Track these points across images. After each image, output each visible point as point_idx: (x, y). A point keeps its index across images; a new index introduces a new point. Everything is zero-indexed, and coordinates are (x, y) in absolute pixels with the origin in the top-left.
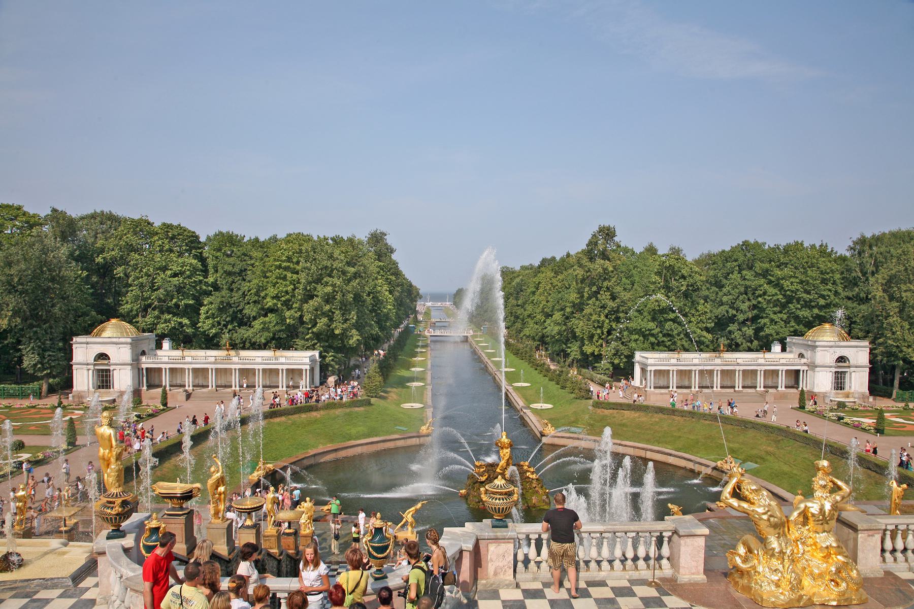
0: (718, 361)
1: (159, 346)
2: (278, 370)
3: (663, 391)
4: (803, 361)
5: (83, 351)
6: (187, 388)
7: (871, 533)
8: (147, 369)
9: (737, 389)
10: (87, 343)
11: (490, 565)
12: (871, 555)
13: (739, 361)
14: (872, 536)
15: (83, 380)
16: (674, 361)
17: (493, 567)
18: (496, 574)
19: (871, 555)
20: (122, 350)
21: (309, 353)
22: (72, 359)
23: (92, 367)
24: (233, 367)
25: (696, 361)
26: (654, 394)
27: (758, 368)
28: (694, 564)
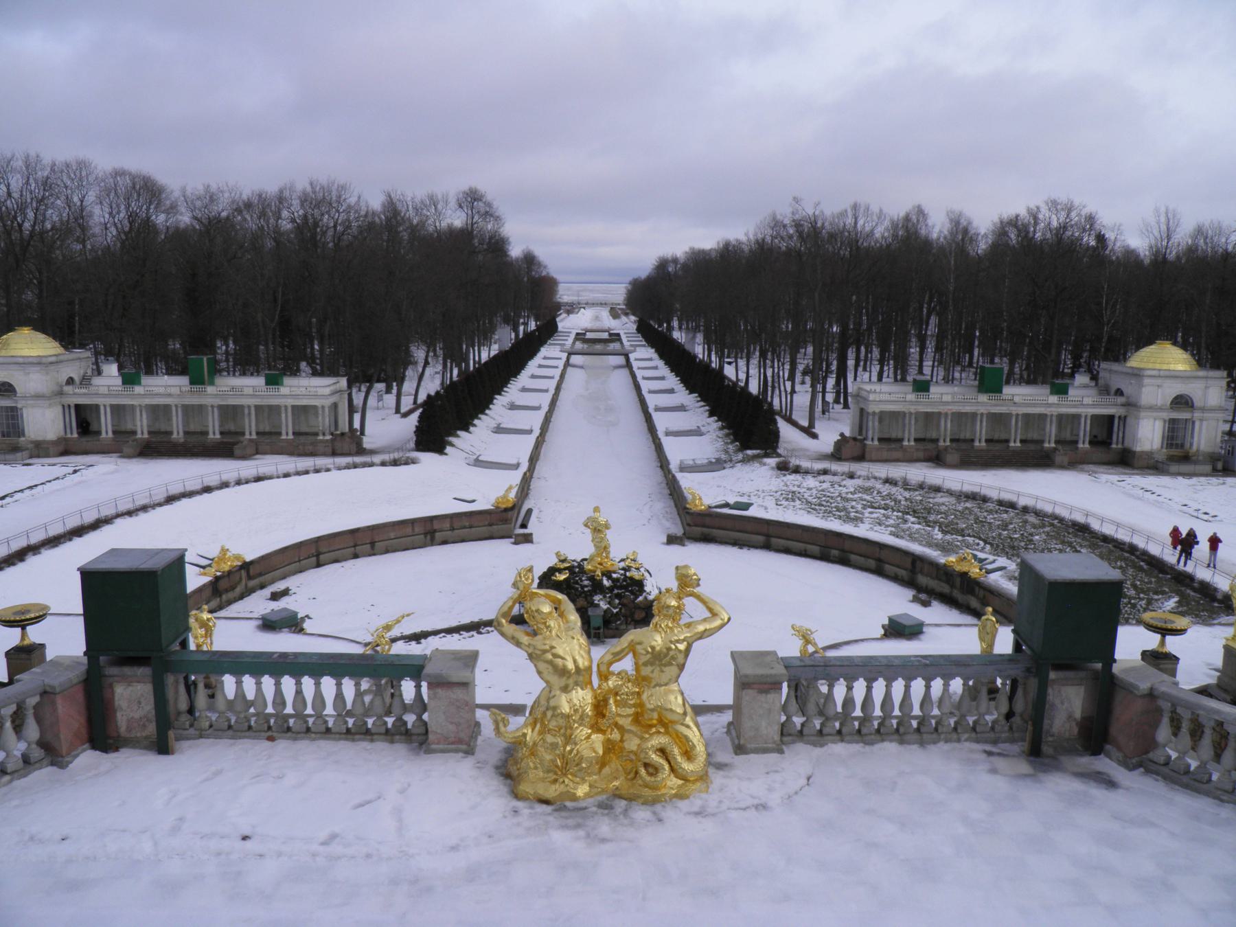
1: (99, 372)
2: (278, 407)
4: (1121, 400)
6: (139, 436)
11: (119, 715)
12: (764, 724)
13: (1016, 399)
14: (766, 692)
17: (125, 718)
18: (129, 729)
19: (764, 724)
25: (946, 398)
28: (452, 727)
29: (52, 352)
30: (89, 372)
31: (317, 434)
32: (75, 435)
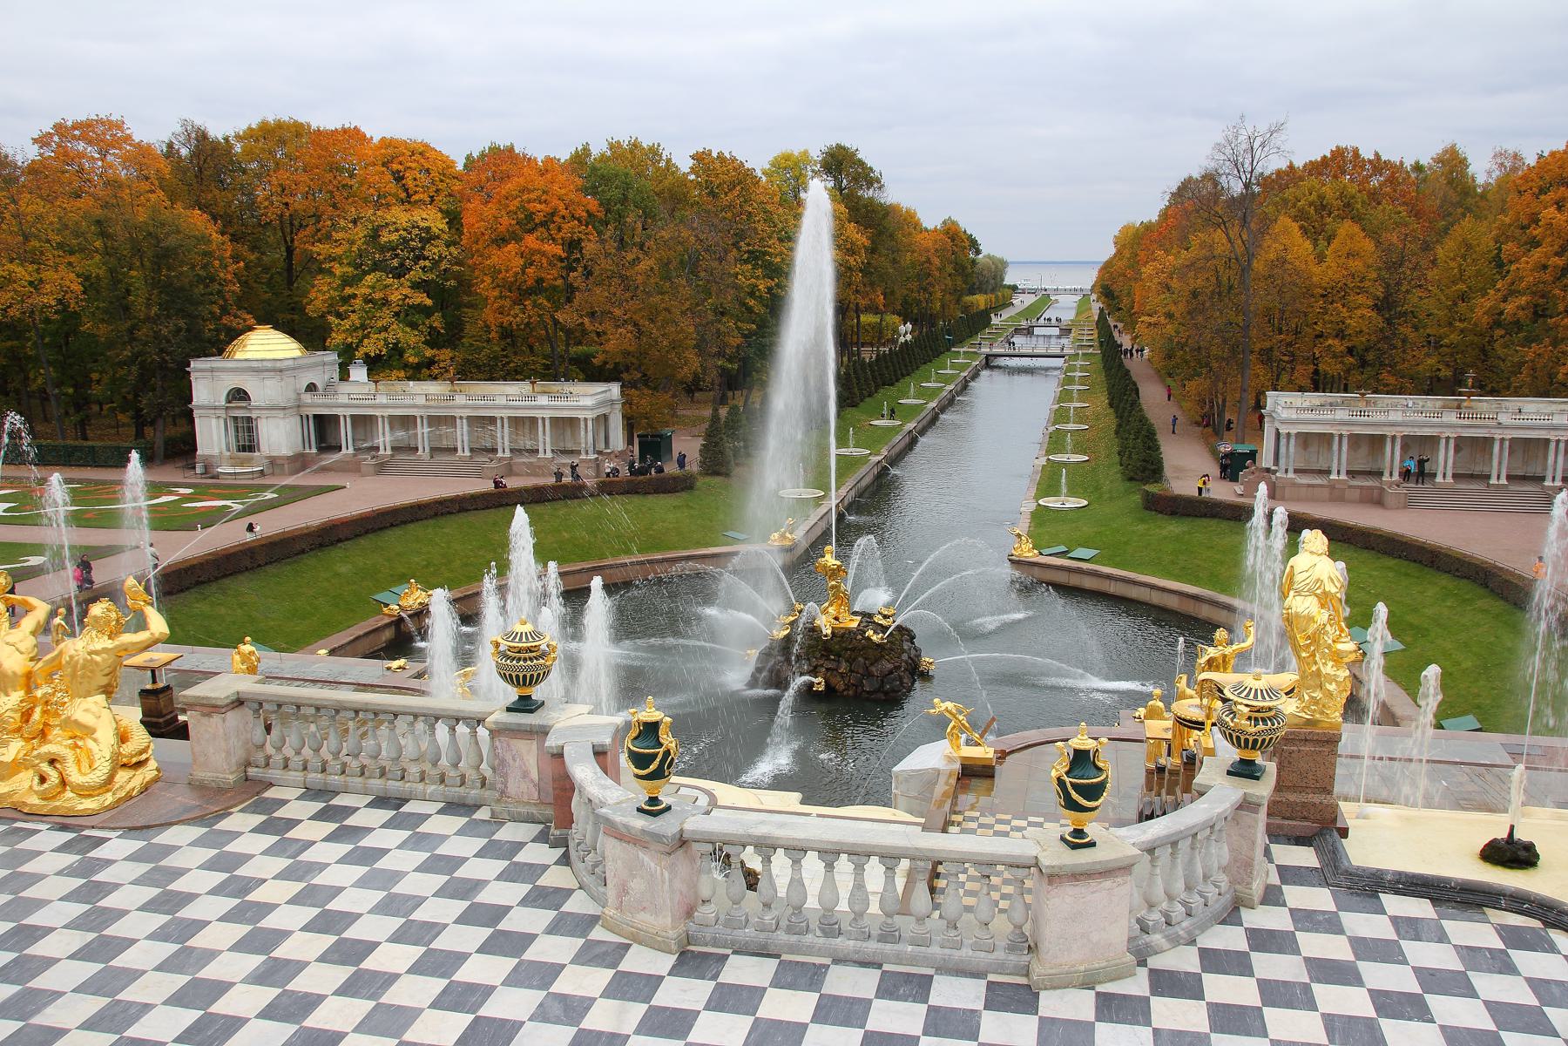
0: (1451, 417)
1: (344, 376)
2: (533, 420)
3: (1318, 481)
5: (208, 385)
7: (206, 710)
8: (315, 416)
9: (1493, 481)
10: (212, 370)
13: (1504, 419)
14: (208, 715)
15: (212, 437)
16: (1341, 415)
20: (267, 382)
21: (599, 387)
22: (190, 400)
23: (222, 413)
24: (457, 413)
26: (1294, 485)
27: (1552, 436)
29: (297, 353)
30: (336, 376)
31: (579, 452)
32: (314, 450)
